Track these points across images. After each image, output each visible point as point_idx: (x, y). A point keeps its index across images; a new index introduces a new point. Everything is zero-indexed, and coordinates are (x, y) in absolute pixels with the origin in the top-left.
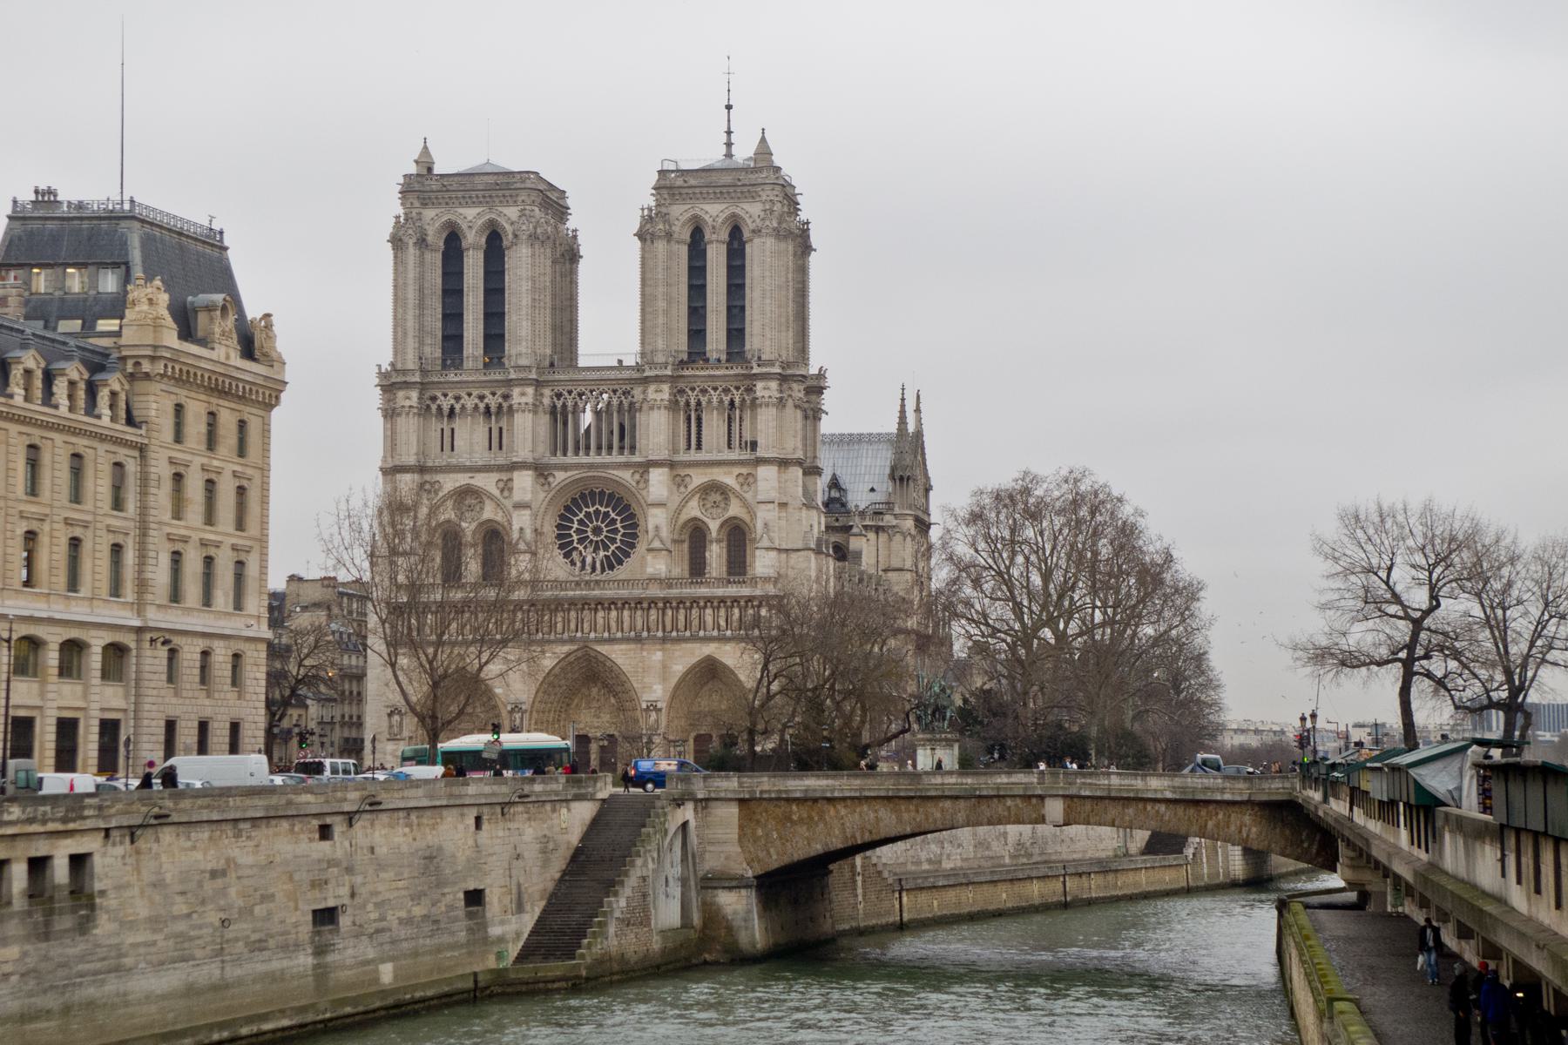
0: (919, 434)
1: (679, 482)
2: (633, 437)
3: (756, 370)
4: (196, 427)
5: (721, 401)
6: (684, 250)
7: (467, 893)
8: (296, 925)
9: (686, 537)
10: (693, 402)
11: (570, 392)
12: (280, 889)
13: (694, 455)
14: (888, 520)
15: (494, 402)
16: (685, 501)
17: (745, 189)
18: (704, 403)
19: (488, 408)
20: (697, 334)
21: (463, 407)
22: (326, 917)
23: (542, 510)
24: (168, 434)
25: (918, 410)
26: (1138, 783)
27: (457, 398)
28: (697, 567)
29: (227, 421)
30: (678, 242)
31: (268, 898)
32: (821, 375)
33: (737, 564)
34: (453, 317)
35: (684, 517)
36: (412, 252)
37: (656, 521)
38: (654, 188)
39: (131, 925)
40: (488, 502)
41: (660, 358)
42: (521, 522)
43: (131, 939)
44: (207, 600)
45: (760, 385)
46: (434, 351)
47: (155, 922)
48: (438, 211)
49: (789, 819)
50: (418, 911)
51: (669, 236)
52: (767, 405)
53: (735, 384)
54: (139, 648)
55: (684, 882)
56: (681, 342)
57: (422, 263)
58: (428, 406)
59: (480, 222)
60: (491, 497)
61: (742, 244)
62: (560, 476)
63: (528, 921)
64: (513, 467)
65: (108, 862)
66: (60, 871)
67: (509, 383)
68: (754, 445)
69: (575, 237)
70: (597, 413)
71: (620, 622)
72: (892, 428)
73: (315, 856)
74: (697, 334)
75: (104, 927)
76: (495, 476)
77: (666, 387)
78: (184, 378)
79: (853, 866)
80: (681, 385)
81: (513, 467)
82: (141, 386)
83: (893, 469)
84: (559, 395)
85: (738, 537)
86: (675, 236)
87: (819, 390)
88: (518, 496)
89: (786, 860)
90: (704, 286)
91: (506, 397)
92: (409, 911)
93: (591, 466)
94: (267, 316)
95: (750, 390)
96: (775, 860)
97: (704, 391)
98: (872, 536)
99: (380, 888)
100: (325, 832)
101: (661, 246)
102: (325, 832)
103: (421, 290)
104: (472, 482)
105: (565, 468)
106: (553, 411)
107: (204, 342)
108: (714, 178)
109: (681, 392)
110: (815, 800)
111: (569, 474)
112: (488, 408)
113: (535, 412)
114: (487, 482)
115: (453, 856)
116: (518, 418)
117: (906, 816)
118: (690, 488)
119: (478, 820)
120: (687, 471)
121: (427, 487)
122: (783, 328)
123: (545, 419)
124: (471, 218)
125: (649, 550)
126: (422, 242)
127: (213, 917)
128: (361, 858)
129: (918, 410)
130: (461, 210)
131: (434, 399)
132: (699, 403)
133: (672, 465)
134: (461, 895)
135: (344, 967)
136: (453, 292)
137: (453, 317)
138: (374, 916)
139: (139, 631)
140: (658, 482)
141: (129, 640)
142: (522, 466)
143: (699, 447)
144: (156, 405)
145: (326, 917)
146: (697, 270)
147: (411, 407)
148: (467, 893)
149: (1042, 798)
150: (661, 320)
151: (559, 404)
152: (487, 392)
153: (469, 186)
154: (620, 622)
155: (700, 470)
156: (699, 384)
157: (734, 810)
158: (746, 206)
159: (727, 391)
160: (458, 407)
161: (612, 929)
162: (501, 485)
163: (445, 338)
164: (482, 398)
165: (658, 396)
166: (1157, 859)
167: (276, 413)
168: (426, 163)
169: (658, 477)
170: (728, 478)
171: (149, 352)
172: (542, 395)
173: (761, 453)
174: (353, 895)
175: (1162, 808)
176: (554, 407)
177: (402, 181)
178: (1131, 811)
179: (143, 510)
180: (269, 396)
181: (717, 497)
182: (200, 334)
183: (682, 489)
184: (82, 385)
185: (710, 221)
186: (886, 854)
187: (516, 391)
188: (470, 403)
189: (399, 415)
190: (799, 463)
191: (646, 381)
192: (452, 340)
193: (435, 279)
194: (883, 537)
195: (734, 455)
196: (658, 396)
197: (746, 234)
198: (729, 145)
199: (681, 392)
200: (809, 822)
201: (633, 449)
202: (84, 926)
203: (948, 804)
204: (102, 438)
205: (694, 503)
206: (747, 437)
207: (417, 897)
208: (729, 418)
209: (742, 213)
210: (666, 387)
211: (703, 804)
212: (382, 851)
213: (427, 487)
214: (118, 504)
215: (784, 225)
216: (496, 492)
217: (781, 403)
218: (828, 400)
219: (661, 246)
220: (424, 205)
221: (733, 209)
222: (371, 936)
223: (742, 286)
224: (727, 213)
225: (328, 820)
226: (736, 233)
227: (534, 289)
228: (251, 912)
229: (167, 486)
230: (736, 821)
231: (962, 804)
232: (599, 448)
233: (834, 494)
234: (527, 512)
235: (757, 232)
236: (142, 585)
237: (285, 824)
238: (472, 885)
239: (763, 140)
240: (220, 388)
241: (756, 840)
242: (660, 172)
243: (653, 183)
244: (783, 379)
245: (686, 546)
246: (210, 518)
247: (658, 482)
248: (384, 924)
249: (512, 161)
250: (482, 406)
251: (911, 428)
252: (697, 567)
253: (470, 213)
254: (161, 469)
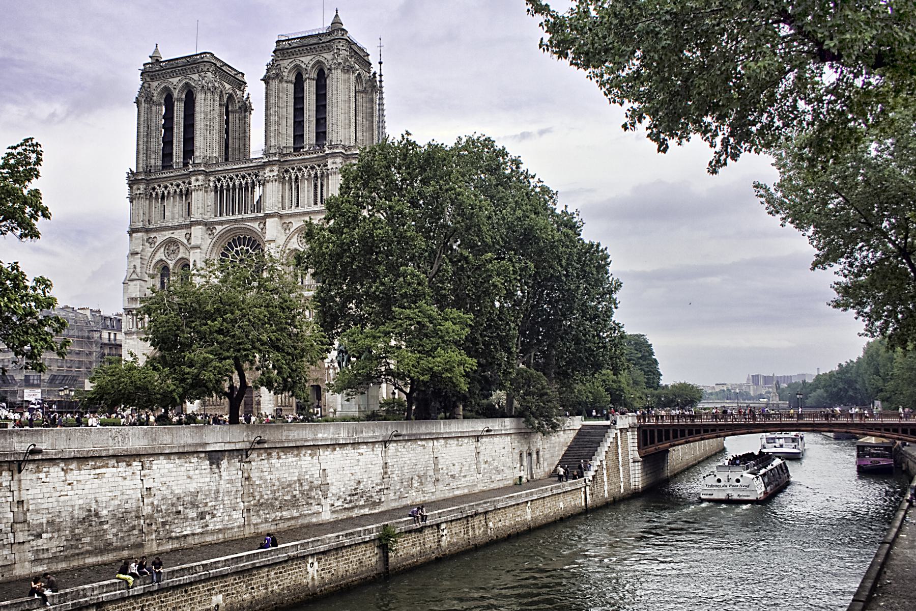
1: (286, 227)
5: (310, 175)
6: (291, 87)
10: (293, 177)
11: (225, 177)
13: (294, 210)
16: (289, 239)
17: (324, 45)
18: (300, 177)
19: (181, 191)
20: (299, 137)
21: (169, 193)
23: (209, 250)
27: (166, 187)
30: (286, 82)
36: (144, 105)
38: (274, 52)
40: (181, 247)
41: (272, 151)
42: (196, 258)
45: (330, 161)
46: (156, 161)
48: (159, 82)
52: (335, 173)
53: (317, 162)
58: (151, 193)
59: (180, 85)
60: (183, 244)
62: (219, 228)
64: (193, 224)
69: (248, 97)
74: (299, 137)
76: (184, 231)
80: (286, 167)
81: (193, 224)
86: (285, 78)
88: (194, 242)
91: (190, 183)
93: (236, 221)
97: (300, 170)
101: (274, 84)
104: (172, 236)
105: (221, 223)
108: (307, 41)
109: (287, 171)
111: (224, 227)
112: (181, 191)
114: (180, 235)
118: (292, 230)
120: (290, 220)
121: (150, 240)
122: (347, 127)
124: (176, 83)
130: (170, 80)
131: (154, 189)
132: (297, 177)
133: (281, 216)
142: (197, 223)
146: (299, 100)
147: (140, 194)
151: (219, 186)
153: (175, 66)
155: (297, 219)
156: (296, 165)
158: (325, 55)
159: (313, 168)
160: (166, 192)
162: (188, 236)
164: (178, 186)
165: (271, 174)
172: (209, 180)
176: (216, 187)
177: (142, 68)
183: (287, 231)
185: (304, 67)
188: (172, 191)
189: (135, 199)
192: (167, 155)
196: (271, 174)
197: (326, 72)
205: (294, 240)
208: (316, 186)
209: (323, 60)
210: (275, 168)
213: (150, 240)
215: (347, 64)
216: (185, 241)
220: (152, 80)
221: (317, 58)
223: (325, 106)
224: (315, 60)
234: (199, 250)
239: (337, 16)
242: (277, 42)
243: (274, 49)
250: (178, 190)
253: (175, 80)
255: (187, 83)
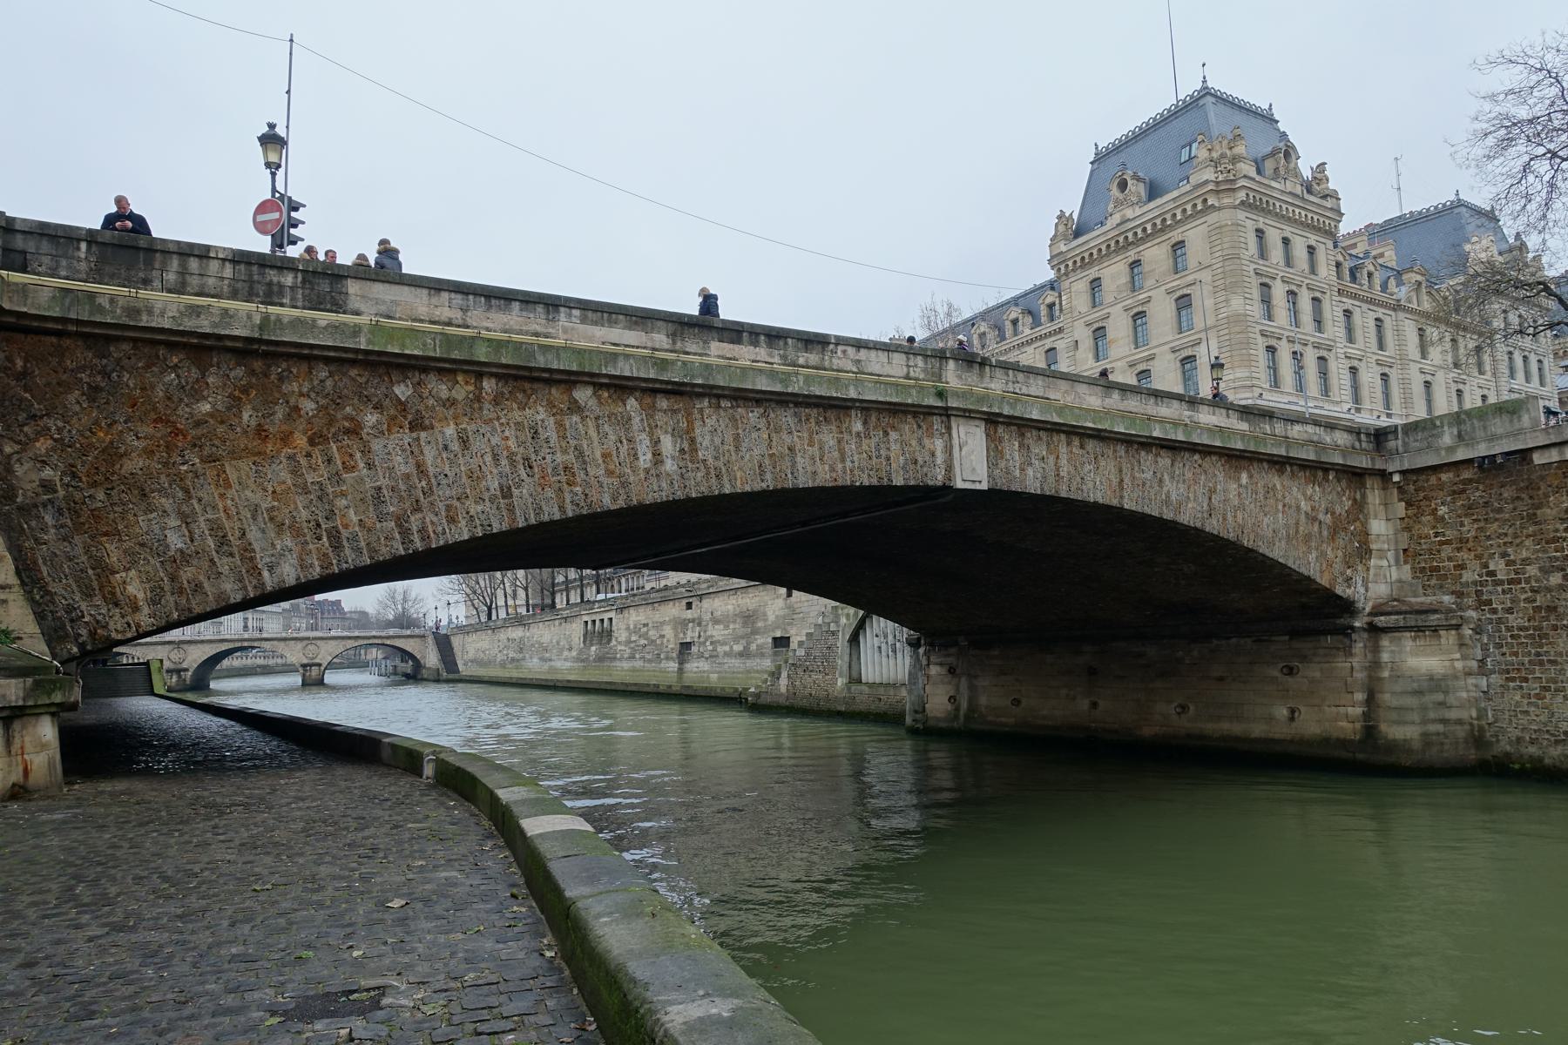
7: (775, 639)
8: (672, 649)
22: (685, 646)
39: (620, 643)
50: (738, 648)
75: (614, 642)
92: (731, 647)
100: (689, 606)
115: (765, 614)
128: (707, 617)
134: (770, 640)
135: (691, 672)
138: (710, 648)
145: (685, 646)
148: (775, 639)
202: (610, 641)
207: (737, 639)
222: (707, 658)
237: (671, 603)
238: (778, 634)
248: (715, 653)
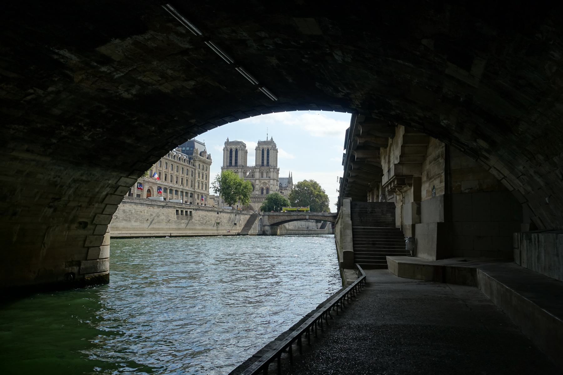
0: (292, 177)
1: (260, 182)
2: (254, 176)
3: (270, 167)
4: (201, 167)
6: (261, 152)
9: (261, 189)
12: (213, 219)
14: (287, 188)
15: (236, 171)
20: (263, 162)
24: (198, 167)
25: (292, 174)
26: (318, 214)
28: (262, 193)
29: (205, 166)
31: (212, 220)
32: (279, 169)
33: (267, 192)
34: (231, 160)
35: (261, 186)
37: (257, 186)
39: (196, 220)
43: (196, 222)
44: (202, 189)
47: (199, 221)
49: (274, 218)
51: (259, 150)
54: (194, 194)
55: (261, 225)
56: (261, 164)
57: (227, 153)
59: (235, 148)
61: (269, 151)
63: (242, 228)
65: (193, 212)
66: (189, 213)
67: (238, 169)
68: (270, 177)
70: (249, 173)
71: (252, 200)
72: (288, 177)
73: (217, 216)
74: (263, 162)
75: (193, 220)
77: (258, 169)
78: (200, 161)
79: (282, 226)
82: (195, 161)
83: (288, 182)
84: (244, 170)
85: (268, 190)
87: (279, 170)
89: (274, 223)
90: (264, 156)
91: (237, 170)
94: (210, 154)
95: (270, 170)
96: (272, 223)
98: (285, 190)
99: (224, 221)
102: (218, 213)
103: (227, 156)
106: (244, 173)
107: (203, 156)
110: (278, 216)
113: (241, 173)
116: (239, 173)
117: (289, 218)
119: (236, 215)
123: (243, 173)
125: (256, 191)
126: (227, 150)
127: (205, 221)
128: (222, 217)
129: (292, 174)
132: (263, 172)
133: (259, 180)
136: (231, 157)
137: (231, 160)
139: (194, 192)
140: (257, 182)
141: (193, 193)
143: (263, 177)
144: (197, 164)
149: (306, 215)
150: (258, 161)
152: (235, 170)
154: (252, 200)
156: (263, 169)
157: (267, 217)
159: (266, 170)
161: (252, 229)
163: (230, 163)
164: (234, 171)
166: (321, 230)
167: (211, 166)
168: (228, 139)
169: (257, 181)
170: (267, 181)
171: (196, 157)
173: (271, 178)
174: (221, 221)
175: (321, 217)
178: (317, 217)
179: (195, 177)
180: (210, 164)
181: (265, 184)
182: (202, 155)
184: (188, 161)
186: (287, 225)
187: (239, 170)
190: (276, 180)
191: (256, 169)
192: (231, 163)
193: (229, 155)
194: (287, 191)
195: (267, 178)
197: (269, 150)
198: (267, 139)
199: (261, 170)
200: (277, 218)
201: (254, 178)
203: (294, 216)
204: (190, 167)
205: (262, 185)
206: (269, 176)
210: (258, 169)
211: (263, 216)
212: (224, 217)
214: (192, 176)
217: (274, 172)
218: (280, 172)
219: (258, 151)
223: (269, 157)
225: (218, 212)
226: (268, 149)
227: (242, 157)
228: (209, 221)
229: (198, 174)
230: (267, 218)
231: (296, 216)
232: (250, 178)
233: (280, 185)
235: (271, 149)
236: (195, 186)
240: (204, 162)
241: (270, 220)
244: (274, 169)
245: (261, 190)
246: (203, 178)
247: (257, 182)
249: (239, 140)
251: (291, 177)
252: (262, 193)
253: (234, 146)
254: (197, 172)
255: (236, 148)
